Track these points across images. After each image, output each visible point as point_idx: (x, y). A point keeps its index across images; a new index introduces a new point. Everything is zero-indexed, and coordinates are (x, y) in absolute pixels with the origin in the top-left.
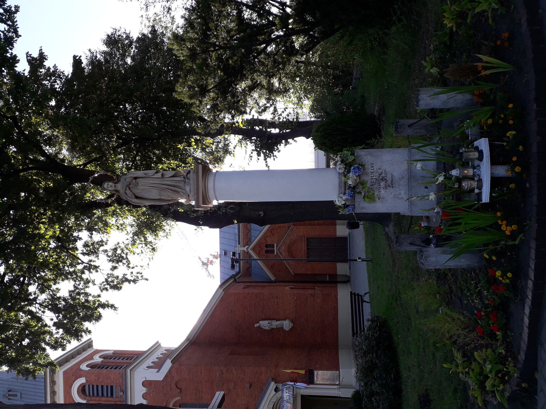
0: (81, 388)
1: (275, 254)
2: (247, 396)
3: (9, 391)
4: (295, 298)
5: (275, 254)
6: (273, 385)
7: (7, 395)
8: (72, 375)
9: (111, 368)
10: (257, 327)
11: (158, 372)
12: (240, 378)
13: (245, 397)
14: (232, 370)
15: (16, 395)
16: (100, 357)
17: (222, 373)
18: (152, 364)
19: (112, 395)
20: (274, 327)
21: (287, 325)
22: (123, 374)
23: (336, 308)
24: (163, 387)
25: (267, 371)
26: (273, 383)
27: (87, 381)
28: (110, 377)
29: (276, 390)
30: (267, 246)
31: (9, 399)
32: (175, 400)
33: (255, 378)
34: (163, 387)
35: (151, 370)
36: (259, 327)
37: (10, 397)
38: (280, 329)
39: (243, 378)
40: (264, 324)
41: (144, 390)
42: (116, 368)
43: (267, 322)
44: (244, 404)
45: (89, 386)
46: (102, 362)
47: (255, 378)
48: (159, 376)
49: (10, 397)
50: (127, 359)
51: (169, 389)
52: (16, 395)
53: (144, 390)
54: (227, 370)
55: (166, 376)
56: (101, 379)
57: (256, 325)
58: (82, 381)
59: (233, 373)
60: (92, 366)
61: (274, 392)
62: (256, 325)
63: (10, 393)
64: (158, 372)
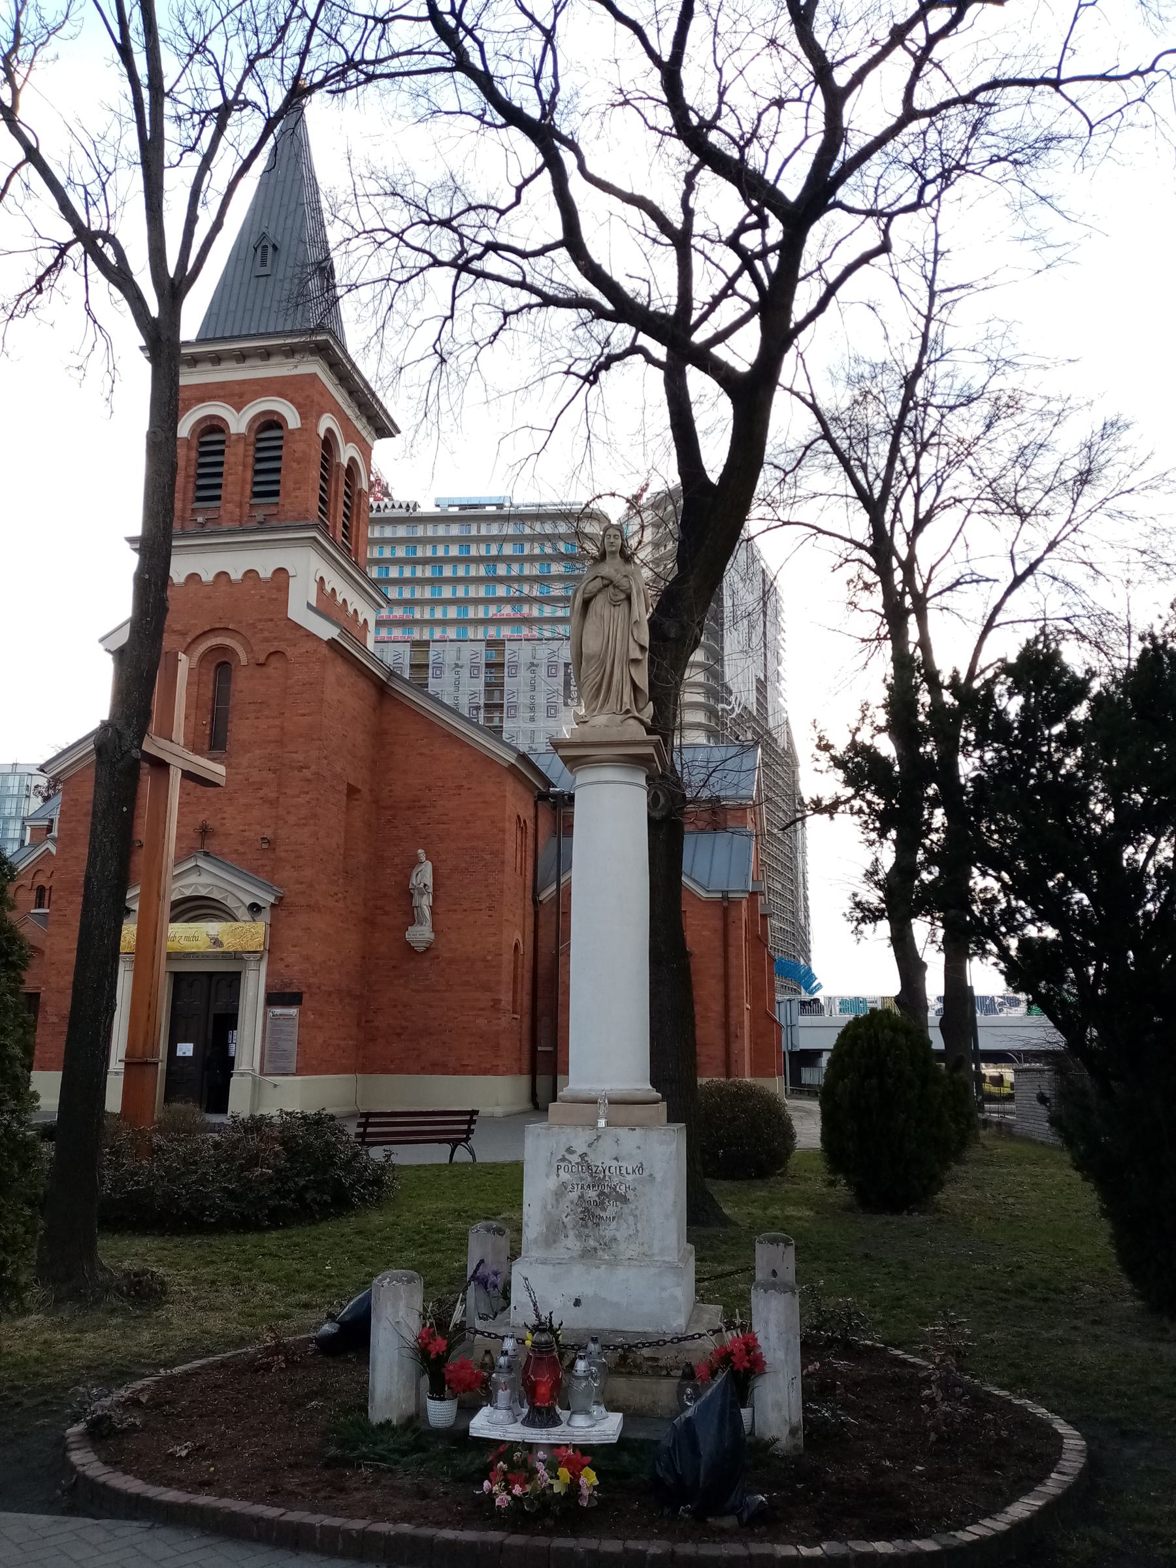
2: (244, 831)
3: (275, 248)
4: (489, 958)
6: (267, 898)
7: (264, 243)
8: (308, 396)
9: (322, 488)
10: (417, 855)
11: (309, 606)
12: (289, 813)
13: (241, 828)
14: (307, 793)
15: (263, 263)
16: (352, 459)
17: (300, 769)
18: (328, 589)
19: (257, 495)
20: (415, 902)
21: (421, 933)
22: (306, 519)
23: (461, 1069)
24: (271, 620)
25: (302, 883)
26: (272, 899)
27: (292, 432)
28: (299, 489)
29: (255, 909)
31: (256, 250)
33: (286, 851)
34: (271, 620)
35: (314, 588)
36: (415, 862)
37: (259, 251)
38: (411, 917)
39: (286, 822)
40: (424, 875)
41: (266, 573)
42: (322, 500)
43: (429, 880)
44: (223, 825)
45: (281, 438)
46: (339, 465)
47: (286, 851)
48: (298, 611)
49: (259, 251)
50: (345, 525)
51: (266, 634)
52: (263, 263)
53: (266, 573)
54: (308, 780)
55: (298, 627)
56: (295, 465)
58: (293, 420)
59: (299, 797)
60: (328, 444)
61: (249, 901)
63: (270, 250)
64: (309, 606)
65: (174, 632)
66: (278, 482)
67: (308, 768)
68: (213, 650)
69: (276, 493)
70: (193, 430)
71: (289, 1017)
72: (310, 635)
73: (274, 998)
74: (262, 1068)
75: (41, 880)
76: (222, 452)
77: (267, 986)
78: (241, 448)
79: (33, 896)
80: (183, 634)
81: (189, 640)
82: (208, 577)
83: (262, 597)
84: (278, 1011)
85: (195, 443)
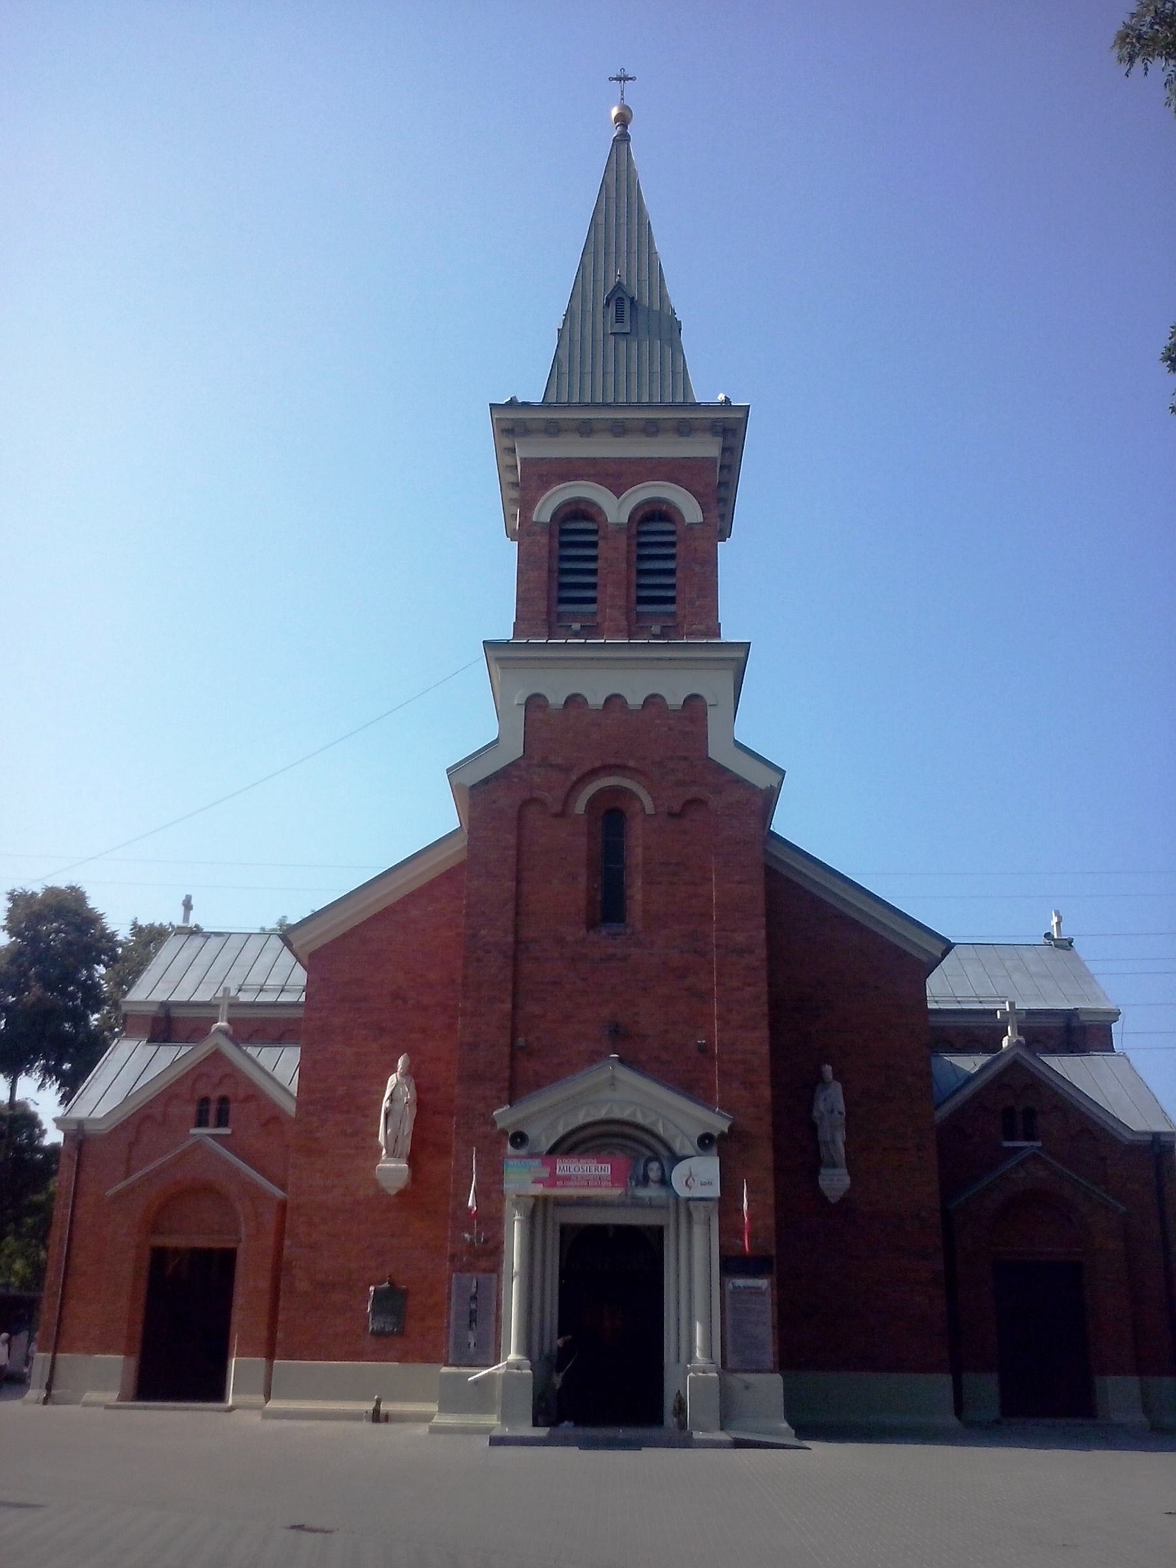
0: (664, 508)
1: (1006, 1144)
2: (667, 1032)
4: (924, 1214)
5: (1006, 1144)
7: (620, 295)
27: (691, 526)
30: (1030, 1114)
32: (643, 794)
34: (685, 758)
36: (818, 1079)
41: (675, 700)
45: (672, 533)
53: (675, 700)
55: (722, 770)
57: (828, 1069)
58: (691, 511)
62: (828, 1069)
63: (627, 304)
65: (551, 766)
66: (672, 587)
67: (752, 952)
68: (602, 792)
69: (671, 600)
70: (554, 516)
71: (756, 1291)
72: (738, 781)
73: (732, 1264)
74: (724, 1363)
75: (203, 1090)
76: (594, 545)
77: (721, 1247)
78: (622, 541)
79: (191, 1110)
80: (565, 769)
81: (574, 778)
82: (635, 700)
83: (670, 729)
84: (741, 1282)
85: (556, 529)
